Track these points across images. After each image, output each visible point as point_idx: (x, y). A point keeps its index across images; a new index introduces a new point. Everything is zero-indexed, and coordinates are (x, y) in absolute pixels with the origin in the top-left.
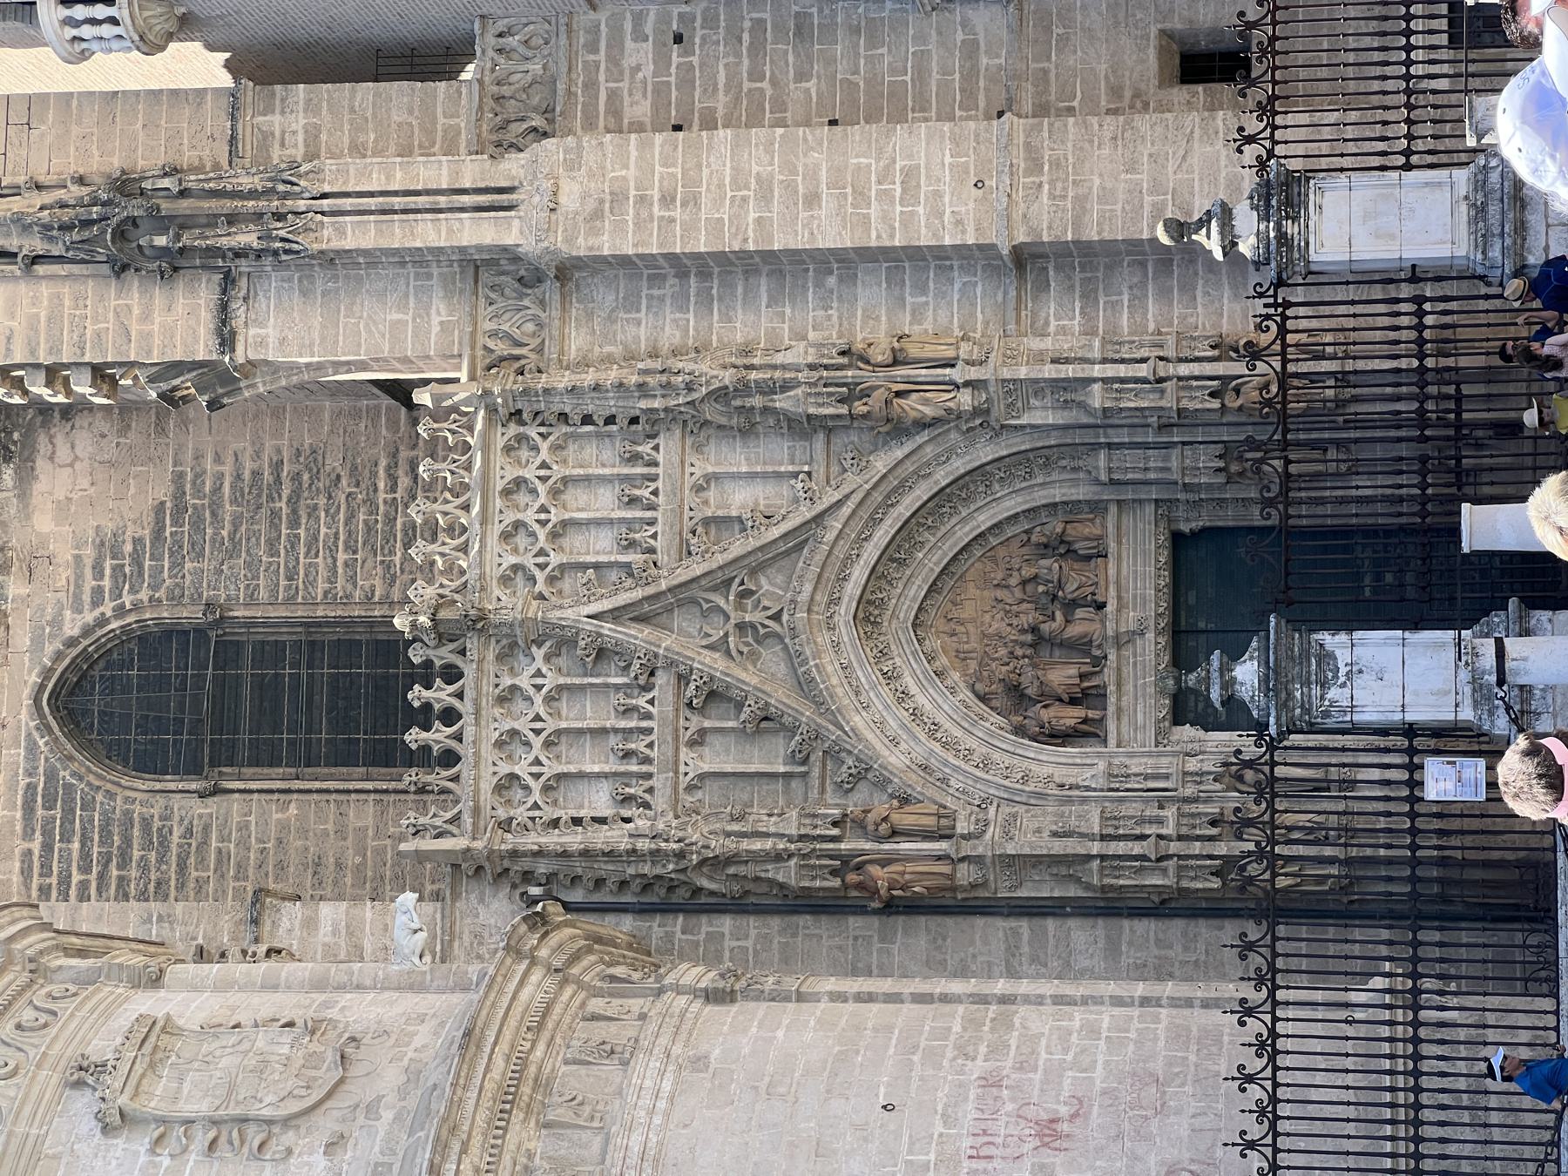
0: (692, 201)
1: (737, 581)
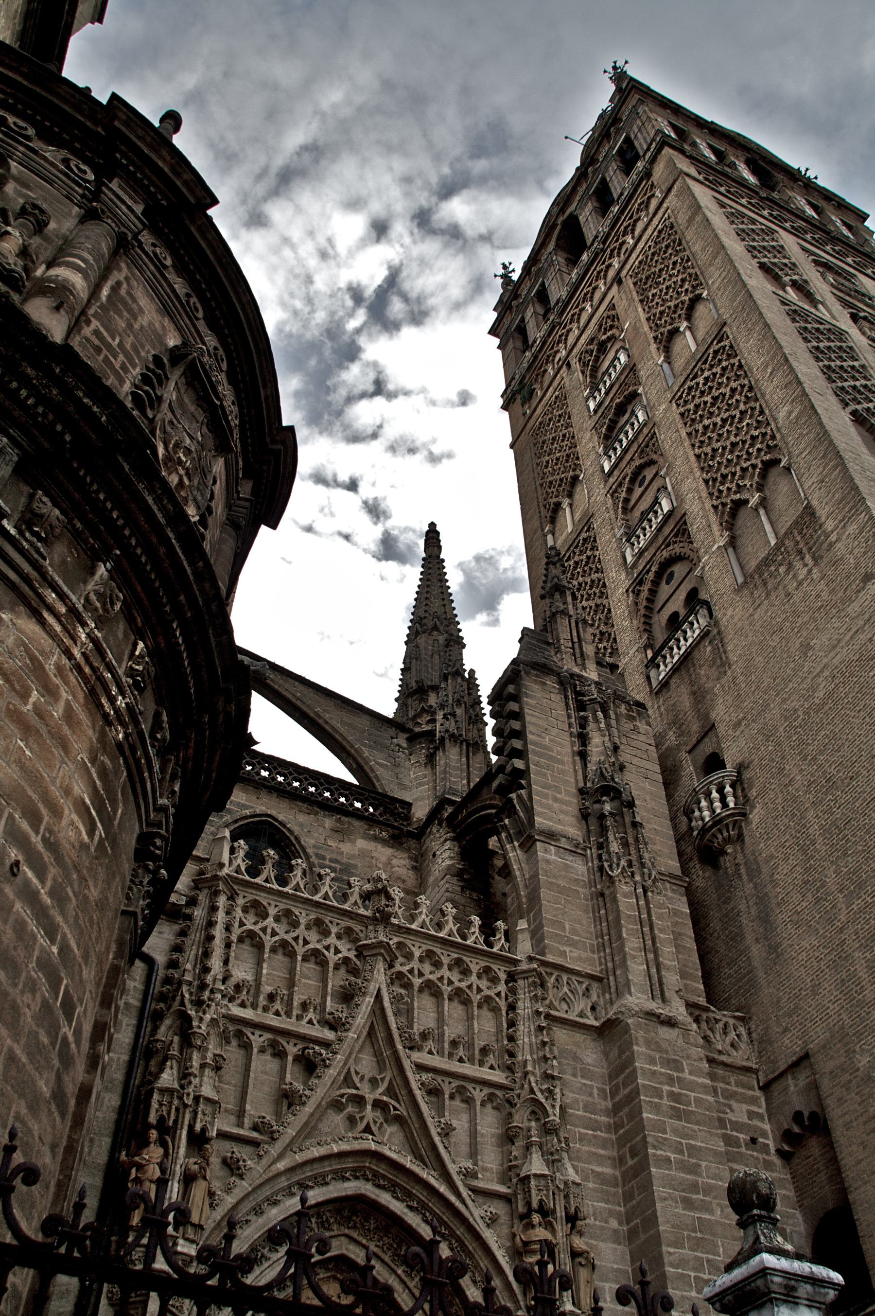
0: (677, 1114)
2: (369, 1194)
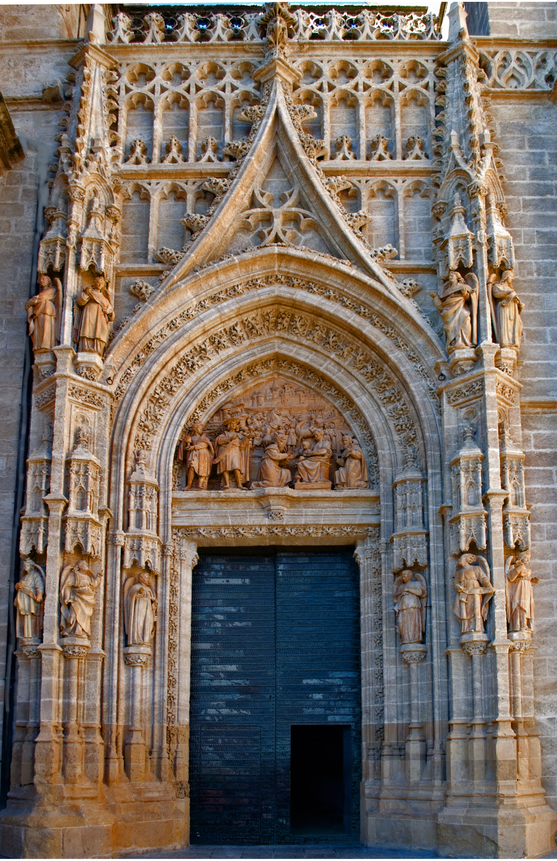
1: (307, 213)
2: (283, 294)
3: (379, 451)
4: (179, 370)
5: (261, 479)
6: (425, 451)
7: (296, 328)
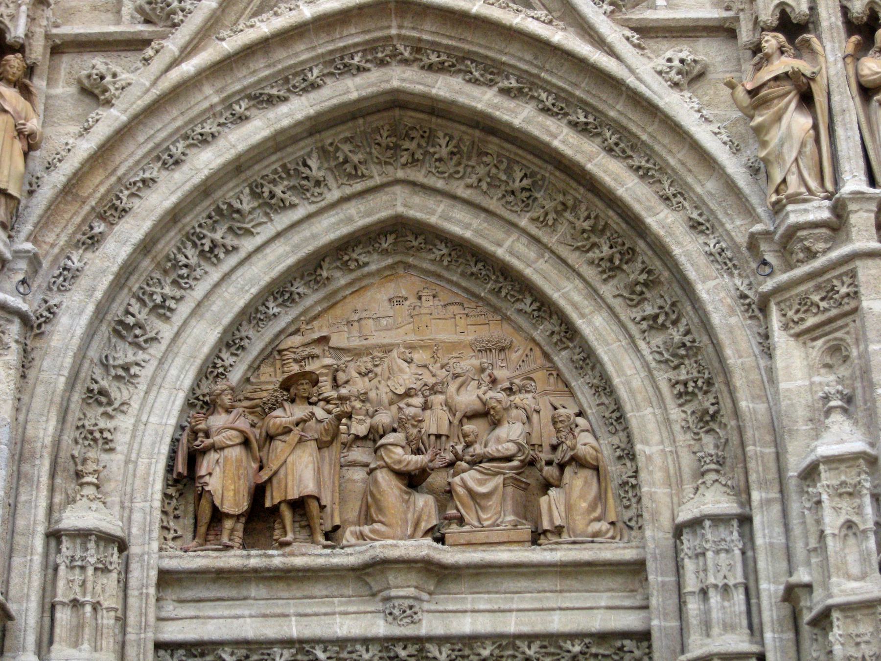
3: (639, 447)
4: (180, 257)
5: (368, 519)
6: (743, 445)
7: (440, 160)
